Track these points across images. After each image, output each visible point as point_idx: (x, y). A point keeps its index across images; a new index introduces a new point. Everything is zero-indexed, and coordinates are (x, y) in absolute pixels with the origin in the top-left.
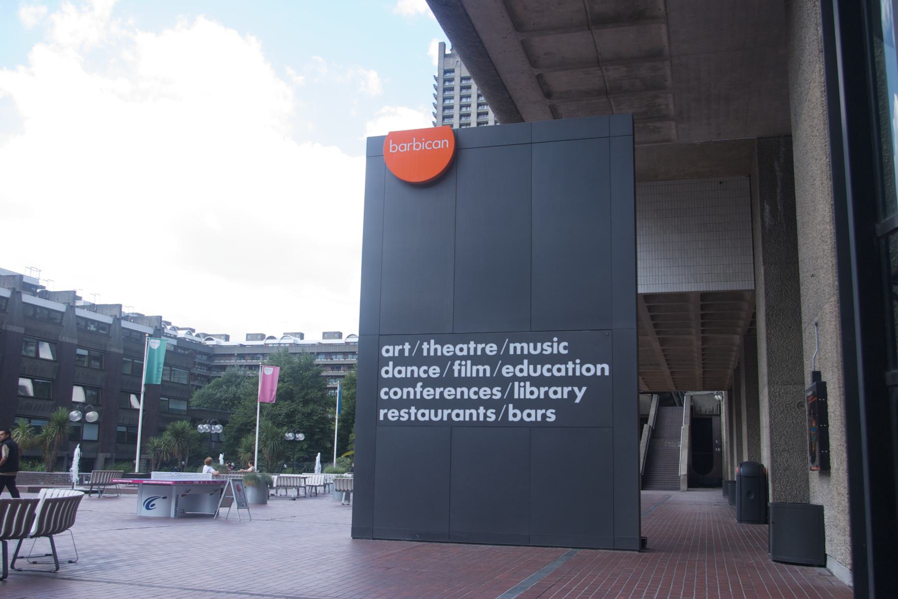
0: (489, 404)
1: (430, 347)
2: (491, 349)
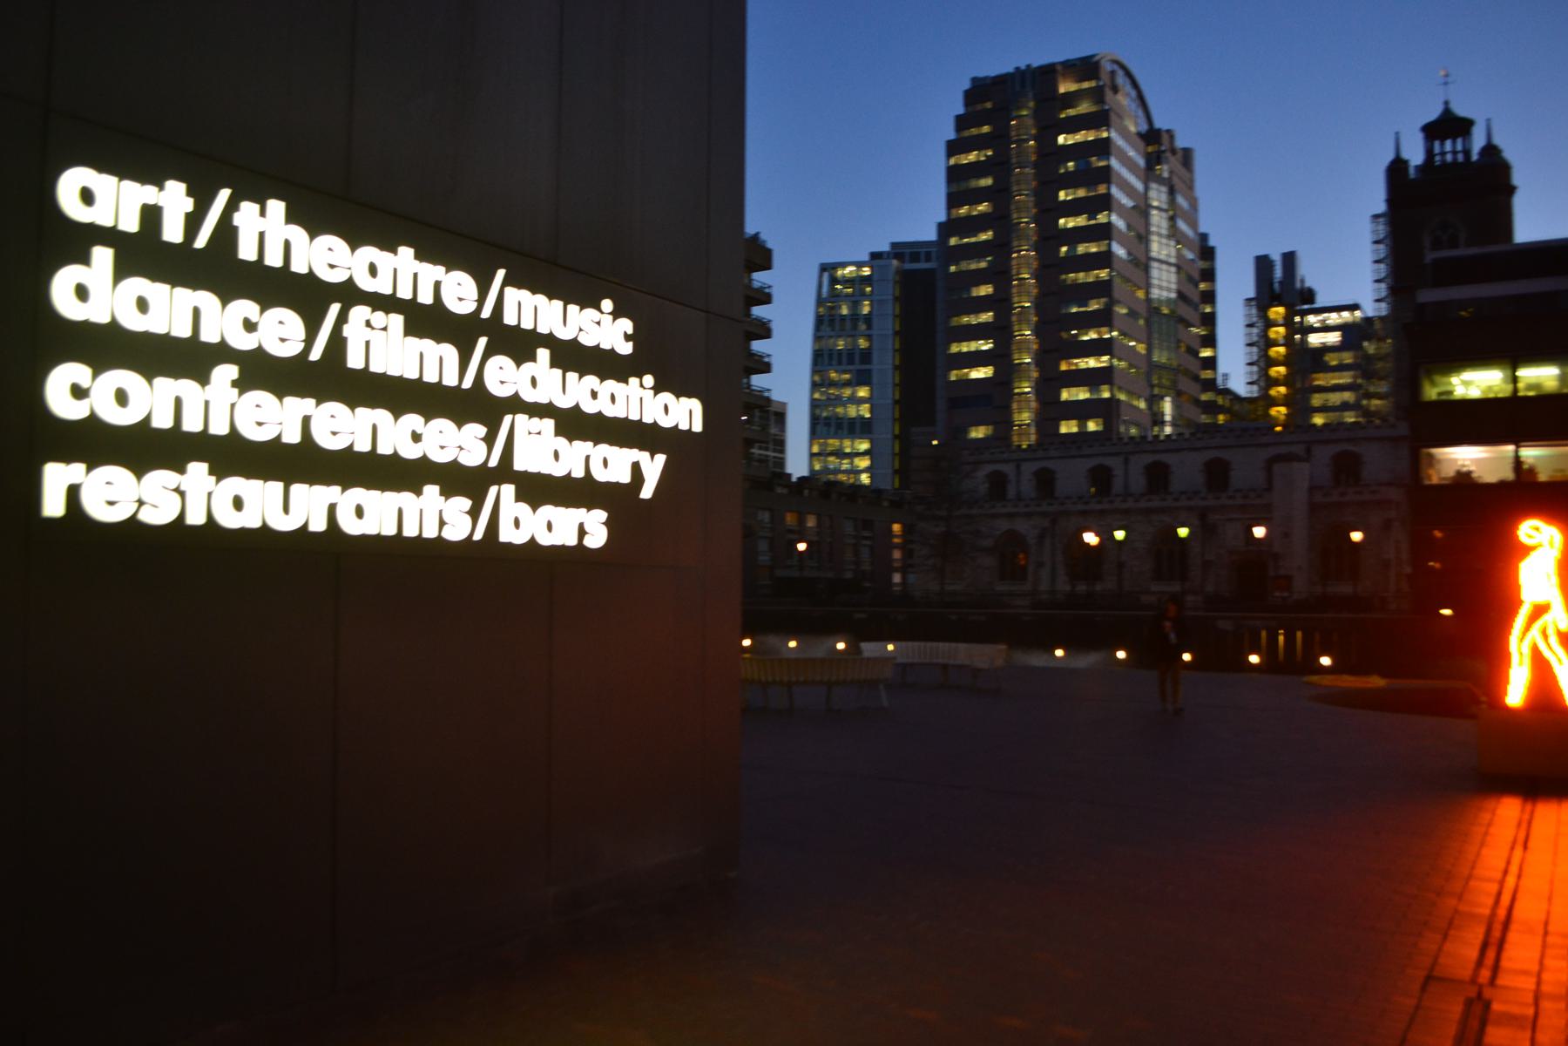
0: (455, 479)
1: (265, 230)
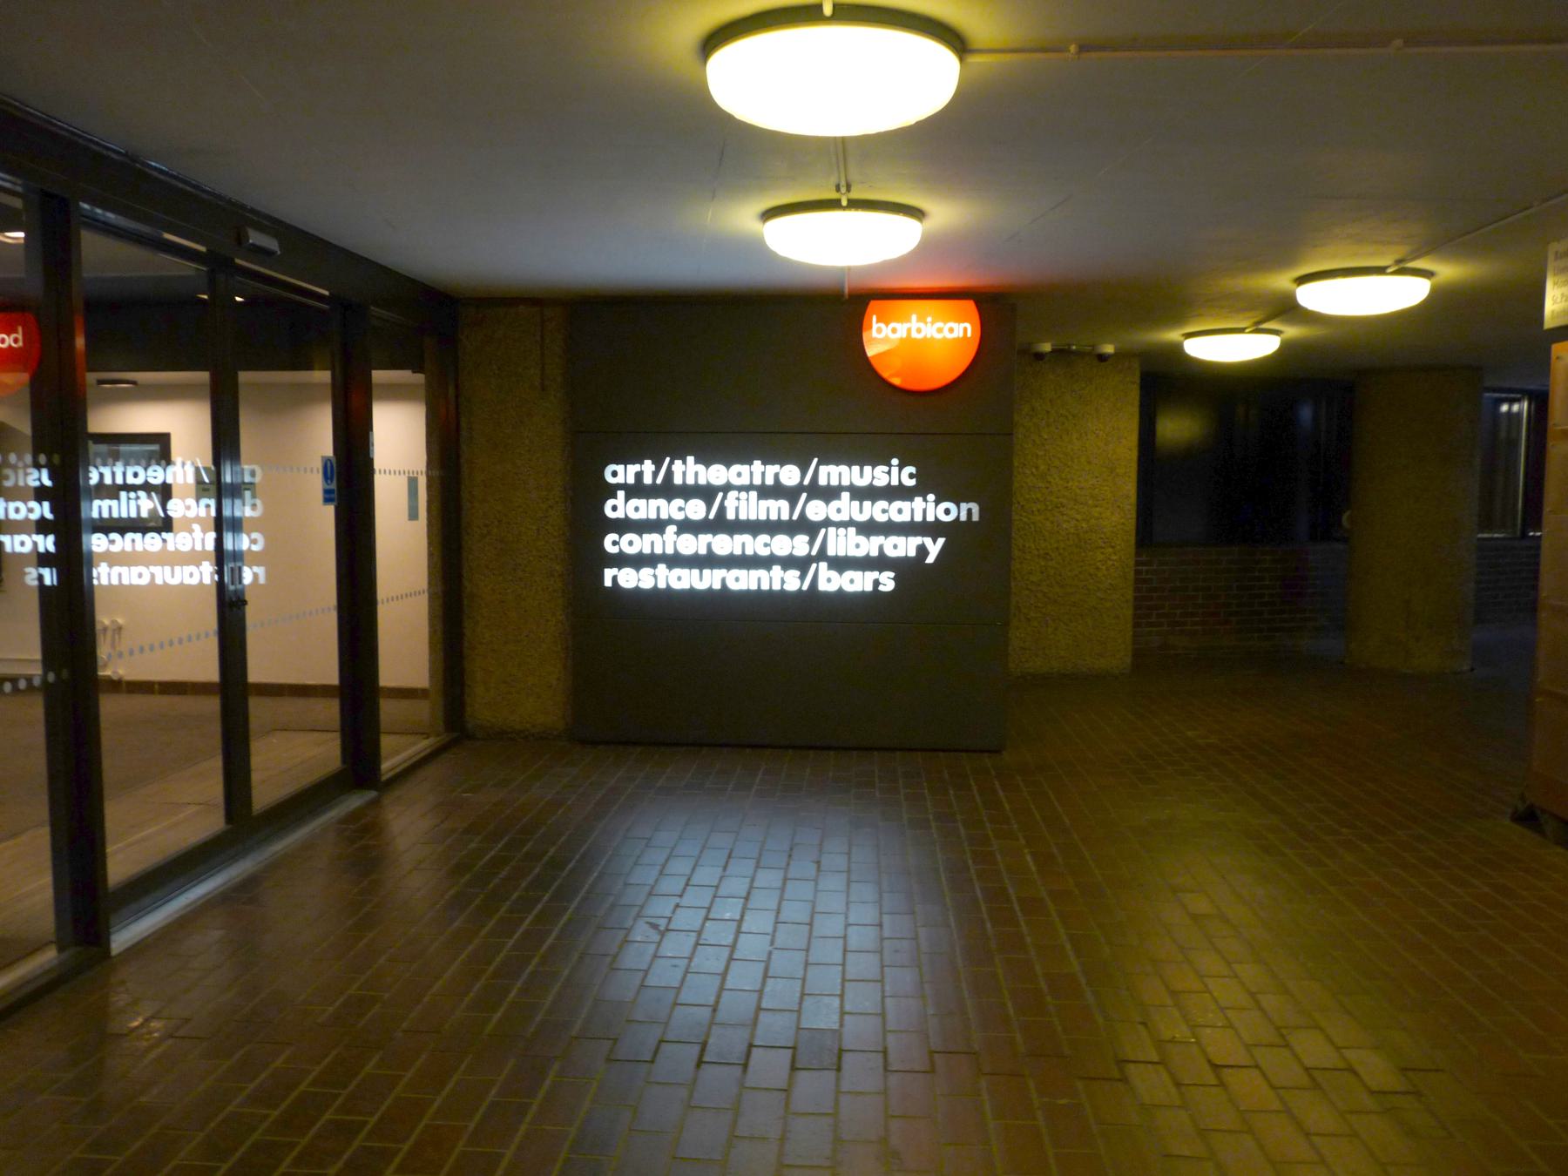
0: (789, 562)
1: (687, 470)
2: (790, 475)
